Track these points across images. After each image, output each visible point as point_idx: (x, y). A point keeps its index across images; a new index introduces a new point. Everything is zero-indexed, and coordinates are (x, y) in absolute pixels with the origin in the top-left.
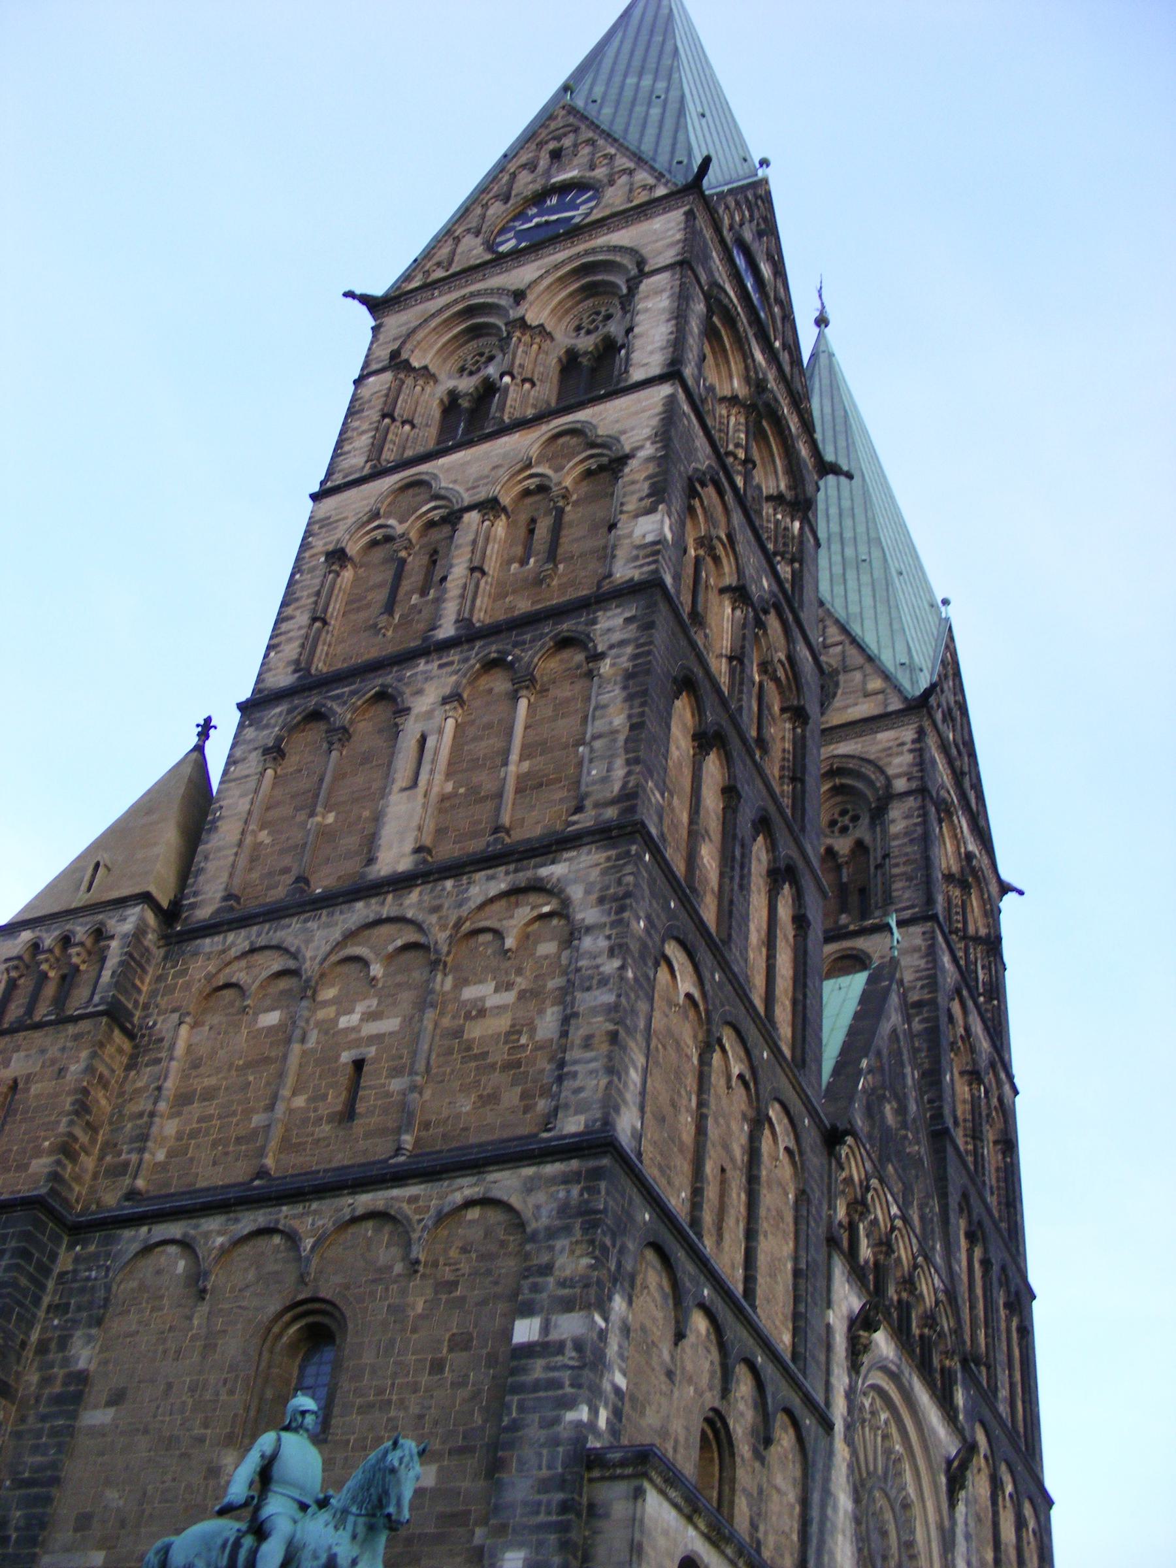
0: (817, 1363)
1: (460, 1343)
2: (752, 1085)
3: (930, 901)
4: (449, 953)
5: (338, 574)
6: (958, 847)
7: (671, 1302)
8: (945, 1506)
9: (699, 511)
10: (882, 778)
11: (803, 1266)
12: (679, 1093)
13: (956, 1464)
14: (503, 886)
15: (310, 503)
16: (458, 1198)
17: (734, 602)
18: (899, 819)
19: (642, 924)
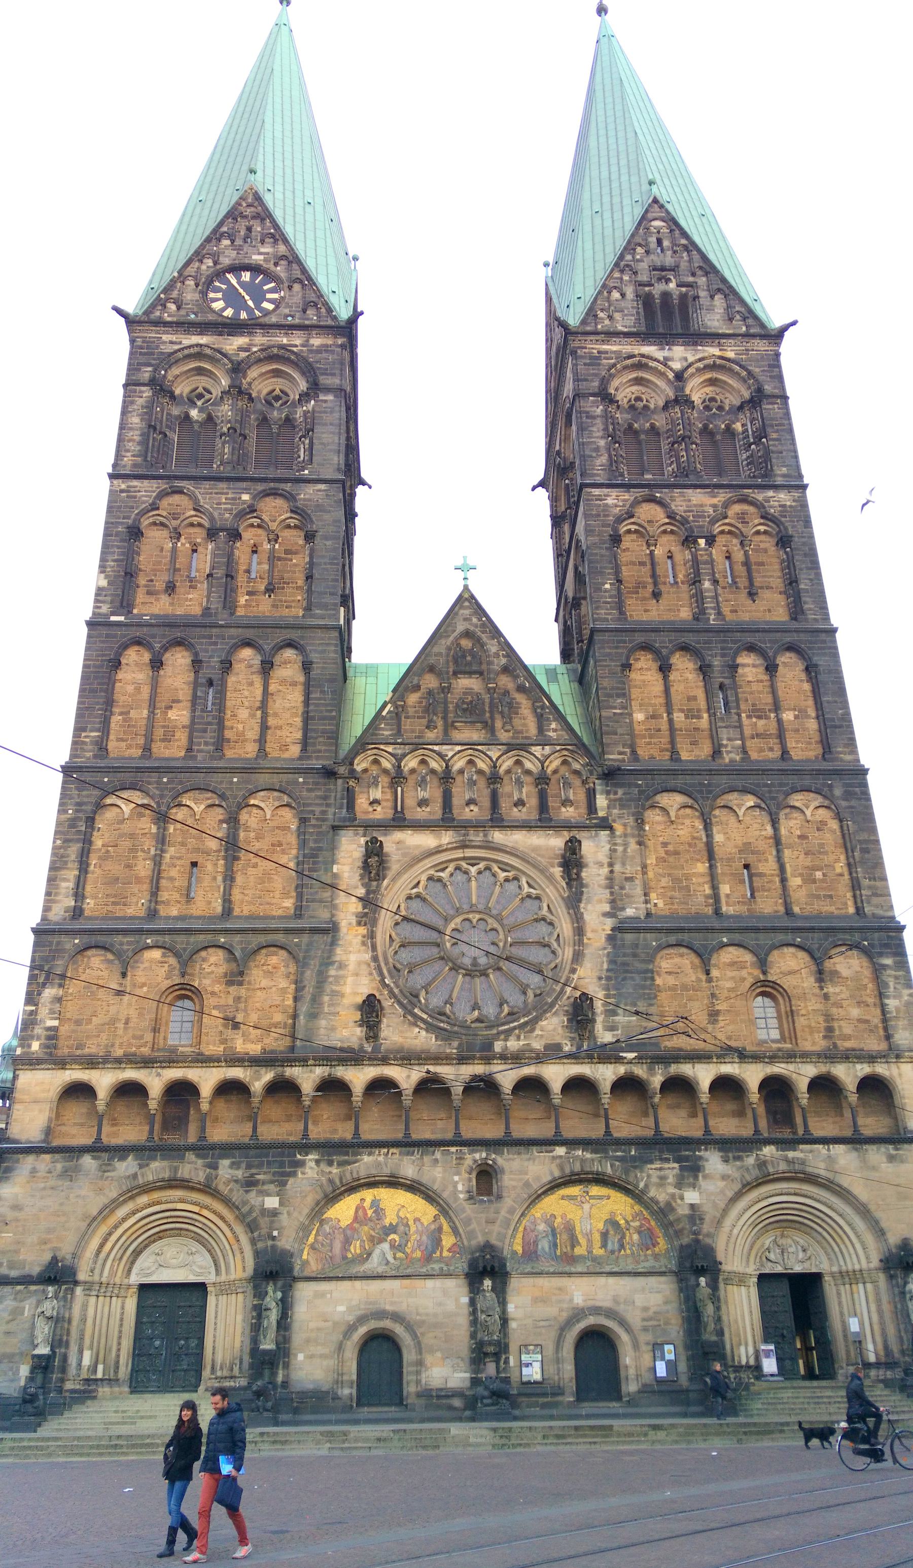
0: (321, 901)
7: (117, 962)
11: (301, 859)
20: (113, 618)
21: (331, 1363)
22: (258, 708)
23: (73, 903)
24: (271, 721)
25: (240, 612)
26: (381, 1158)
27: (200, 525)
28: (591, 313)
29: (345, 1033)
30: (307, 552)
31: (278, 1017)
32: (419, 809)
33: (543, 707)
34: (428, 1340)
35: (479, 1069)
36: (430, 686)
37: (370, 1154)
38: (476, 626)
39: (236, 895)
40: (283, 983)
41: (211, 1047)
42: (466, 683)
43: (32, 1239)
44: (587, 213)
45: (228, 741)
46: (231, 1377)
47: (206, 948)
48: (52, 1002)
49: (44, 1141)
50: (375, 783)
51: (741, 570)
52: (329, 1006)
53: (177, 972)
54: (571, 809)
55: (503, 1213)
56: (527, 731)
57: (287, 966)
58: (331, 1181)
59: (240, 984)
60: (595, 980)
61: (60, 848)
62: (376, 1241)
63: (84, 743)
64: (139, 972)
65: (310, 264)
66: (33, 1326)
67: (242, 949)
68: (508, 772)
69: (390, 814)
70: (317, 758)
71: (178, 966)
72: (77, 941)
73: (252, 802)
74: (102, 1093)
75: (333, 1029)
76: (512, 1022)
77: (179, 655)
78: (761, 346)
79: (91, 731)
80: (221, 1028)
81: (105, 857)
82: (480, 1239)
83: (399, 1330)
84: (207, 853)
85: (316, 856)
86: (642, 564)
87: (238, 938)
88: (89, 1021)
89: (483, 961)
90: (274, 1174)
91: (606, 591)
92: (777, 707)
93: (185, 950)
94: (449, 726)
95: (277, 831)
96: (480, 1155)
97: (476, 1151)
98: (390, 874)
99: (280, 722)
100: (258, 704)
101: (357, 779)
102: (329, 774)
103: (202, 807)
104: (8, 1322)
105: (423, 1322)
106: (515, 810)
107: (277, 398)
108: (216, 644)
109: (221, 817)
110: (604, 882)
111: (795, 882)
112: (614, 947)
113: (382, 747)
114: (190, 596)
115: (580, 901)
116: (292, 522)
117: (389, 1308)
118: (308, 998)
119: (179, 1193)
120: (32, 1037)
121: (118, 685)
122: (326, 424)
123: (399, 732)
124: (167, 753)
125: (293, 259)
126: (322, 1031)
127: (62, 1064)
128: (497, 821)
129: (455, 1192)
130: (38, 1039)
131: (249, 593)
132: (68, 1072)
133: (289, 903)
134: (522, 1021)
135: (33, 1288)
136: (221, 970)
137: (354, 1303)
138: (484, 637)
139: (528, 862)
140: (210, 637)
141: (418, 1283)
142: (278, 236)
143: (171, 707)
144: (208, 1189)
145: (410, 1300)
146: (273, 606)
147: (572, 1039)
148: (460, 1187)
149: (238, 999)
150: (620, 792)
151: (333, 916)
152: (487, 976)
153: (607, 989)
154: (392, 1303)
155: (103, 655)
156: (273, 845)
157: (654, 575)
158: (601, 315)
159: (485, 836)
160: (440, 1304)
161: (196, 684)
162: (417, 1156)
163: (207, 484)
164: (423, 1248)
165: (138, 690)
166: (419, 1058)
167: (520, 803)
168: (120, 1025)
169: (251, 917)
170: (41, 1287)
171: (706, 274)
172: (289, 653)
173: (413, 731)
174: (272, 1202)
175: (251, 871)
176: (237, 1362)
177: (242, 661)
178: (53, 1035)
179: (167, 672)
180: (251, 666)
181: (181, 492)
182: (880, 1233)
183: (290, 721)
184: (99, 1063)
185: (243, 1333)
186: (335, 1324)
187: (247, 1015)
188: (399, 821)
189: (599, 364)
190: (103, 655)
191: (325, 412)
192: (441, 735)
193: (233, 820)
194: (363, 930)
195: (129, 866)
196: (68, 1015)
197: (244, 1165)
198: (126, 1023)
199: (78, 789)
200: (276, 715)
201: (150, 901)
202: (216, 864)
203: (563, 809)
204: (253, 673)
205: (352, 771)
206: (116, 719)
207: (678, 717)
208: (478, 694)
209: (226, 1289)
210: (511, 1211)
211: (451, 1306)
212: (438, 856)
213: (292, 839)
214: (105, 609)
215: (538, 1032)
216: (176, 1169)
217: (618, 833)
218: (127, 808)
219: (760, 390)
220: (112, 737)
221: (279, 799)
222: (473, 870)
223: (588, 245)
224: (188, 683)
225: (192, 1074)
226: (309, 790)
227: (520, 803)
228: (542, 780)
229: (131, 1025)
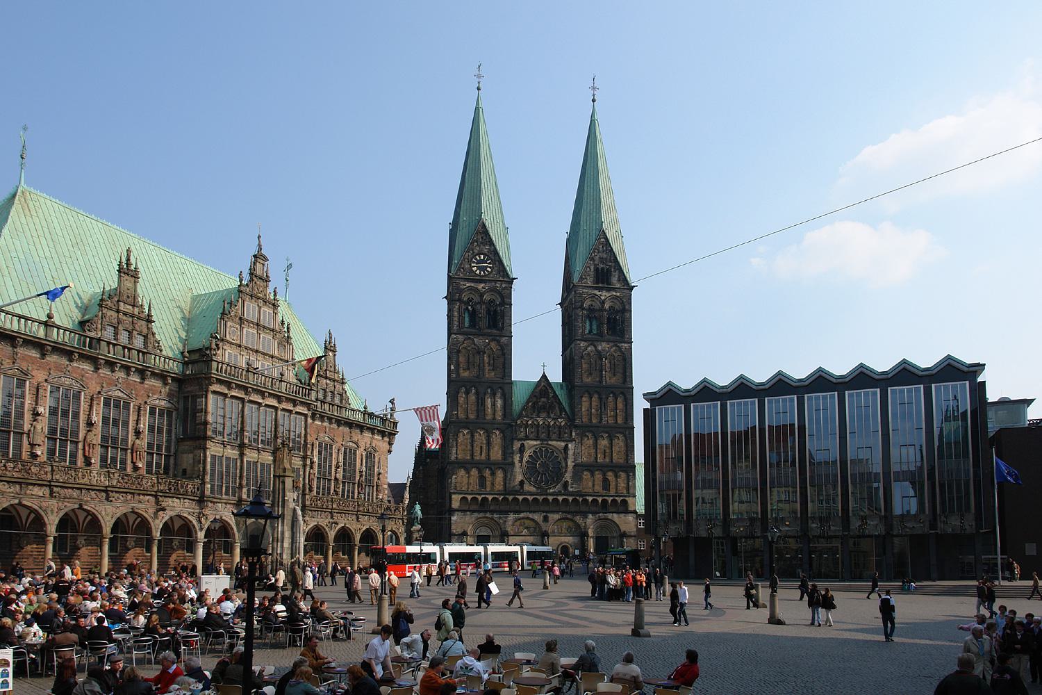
8: (564, 454)
25: (487, 376)
28: (581, 278)
35: (545, 497)
39: (491, 454)
42: (543, 399)
44: (582, 229)
51: (613, 366)
65: (501, 254)
78: (627, 291)
82: (544, 530)
92: (616, 410)
94: (539, 412)
107: (492, 302)
111: (614, 454)
125: (496, 253)
127: (461, 494)
142: (491, 243)
169: (495, 460)
171: (615, 262)
181: (470, 338)
182: (620, 530)
188: (527, 438)
207: (593, 410)
219: (625, 308)
223: (581, 246)
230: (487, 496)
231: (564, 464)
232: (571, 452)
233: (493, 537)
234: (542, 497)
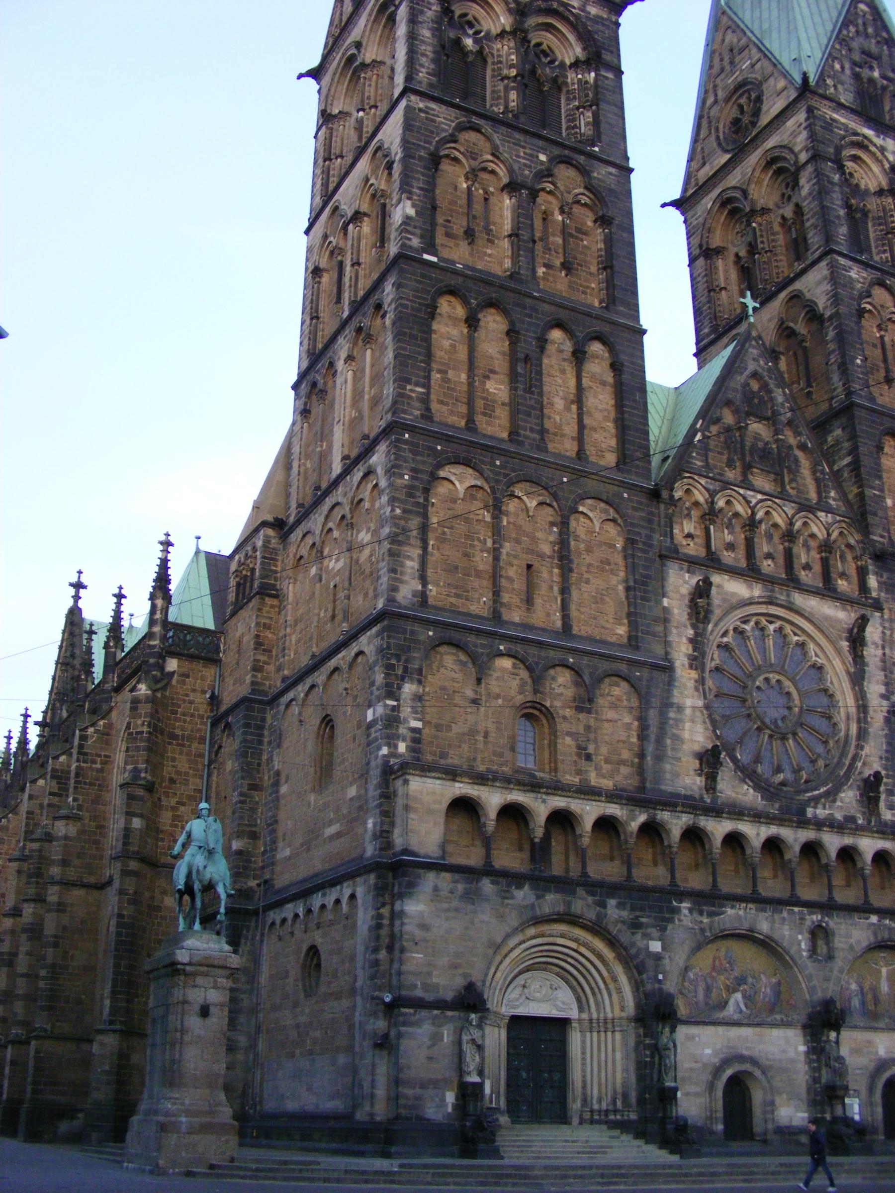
0: (654, 635)
1: (359, 727)
2: (555, 504)
3: (828, 238)
4: (352, 518)
5: (319, 283)
6: (883, 166)
7: (470, 665)
9: (460, 157)
10: (793, 157)
11: (631, 583)
12: (472, 546)
13: (855, 630)
14: (361, 474)
15: (305, 237)
16: (353, 654)
17: (509, 193)
18: (806, 184)
19: (406, 477)
20: (426, 257)
21: (703, 1100)
22: (572, 402)
23: (420, 587)
24: (587, 421)
26: (741, 912)
27: (493, 172)
28: (821, 78)
29: (688, 781)
30: (600, 238)
31: (626, 755)
32: (725, 553)
33: (822, 472)
34: (777, 1083)
36: (725, 421)
37: (733, 907)
38: (763, 369)
39: (574, 613)
40: (628, 719)
41: (568, 777)
43: (444, 961)
45: (547, 431)
46: (615, 1111)
47: (554, 666)
48: (413, 700)
49: (443, 858)
50: (688, 516)
52: (673, 749)
53: (529, 688)
54: (845, 583)
55: (836, 972)
56: (808, 493)
57: (629, 700)
58: (702, 930)
59: (589, 711)
60: (877, 759)
61: (400, 518)
62: (731, 990)
63: (410, 397)
64: (494, 682)
66: (460, 1055)
67: (591, 674)
68: (798, 531)
69: (702, 552)
70: (637, 474)
71: (529, 681)
72: (431, 633)
73: (581, 509)
74: (492, 812)
75: (677, 775)
76: (815, 789)
77: (490, 318)
79: (417, 385)
80: (575, 758)
81: (442, 539)
82: (819, 995)
83: (757, 1073)
84: (541, 556)
85: (645, 584)
86: (874, 346)
87: (585, 661)
88: (449, 728)
89: (780, 723)
90: (655, 918)
91: (858, 366)
93: (537, 664)
94: (747, 468)
95: (604, 548)
96: (816, 917)
97: (813, 913)
98: (714, 618)
99: (595, 424)
100: (571, 397)
101: (676, 506)
102: (655, 494)
103: (535, 503)
104: (429, 1047)
105: (771, 1067)
106: (803, 573)
107: (543, 52)
108: (530, 316)
109: (551, 519)
110: (880, 664)
112: (890, 729)
113: (696, 477)
114: (489, 251)
115: (863, 678)
116: (584, 199)
117: (745, 1052)
118: (653, 737)
119: (562, 928)
120: (397, 737)
121: (434, 336)
122: (609, 103)
123: (707, 465)
124: (490, 430)
126: (668, 776)
127: (452, 774)
128: (792, 581)
129: (800, 950)
130: (404, 740)
131: (546, 266)
132: (457, 785)
133: (622, 630)
134: (822, 790)
135: (449, 1013)
136: (570, 693)
137: (719, 1046)
138: (772, 384)
139: (821, 631)
140: (525, 307)
141: (766, 1031)
143: (488, 377)
144: (597, 929)
145: (761, 1046)
146: (570, 287)
147: (864, 814)
148: (803, 946)
149: (588, 728)
150: (885, 575)
151: (667, 653)
152: (787, 739)
153: (886, 769)
154: (748, 1048)
155: (420, 298)
156: (602, 562)
157: (885, 360)
158: (829, 81)
159: (788, 595)
160: (784, 1051)
161: (513, 360)
162: (768, 914)
163: (503, 130)
164: (767, 999)
165: (453, 346)
166: (767, 817)
167: (807, 567)
168: (480, 738)
169: (591, 640)
170: (456, 1013)
172: (596, 347)
173: (715, 467)
174: (656, 946)
175: (584, 587)
176: (619, 1096)
177: (553, 342)
178: (416, 737)
179: (481, 334)
180: (562, 351)
183: (603, 425)
184: (488, 779)
185: (626, 1070)
186: (705, 1065)
187: (597, 748)
189: (832, 131)
190: (420, 298)
191: (607, 90)
192: (740, 478)
193: (564, 524)
194: (694, 674)
195: (467, 555)
196: (428, 717)
197: (628, 906)
198: (486, 737)
199: (411, 451)
200: (589, 413)
201: (495, 602)
202: (551, 572)
203: (840, 582)
204: (564, 360)
205: (672, 497)
206: (436, 376)
208: (767, 444)
209: (605, 1025)
210: (841, 971)
211: (792, 1054)
212: (747, 608)
213: (619, 559)
214: (415, 242)
215: (838, 803)
216: (568, 904)
217: (886, 617)
218: (461, 488)
220: (433, 397)
221: (606, 512)
222: (772, 627)
224: (504, 354)
225: (576, 805)
226: (635, 509)
227: (807, 567)
228: (826, 547)
229: (490, 739)
230: (576, 805)
231: (847, 700)
232: (872, 654)
233: (592, 1025)
234: (807, 835)
